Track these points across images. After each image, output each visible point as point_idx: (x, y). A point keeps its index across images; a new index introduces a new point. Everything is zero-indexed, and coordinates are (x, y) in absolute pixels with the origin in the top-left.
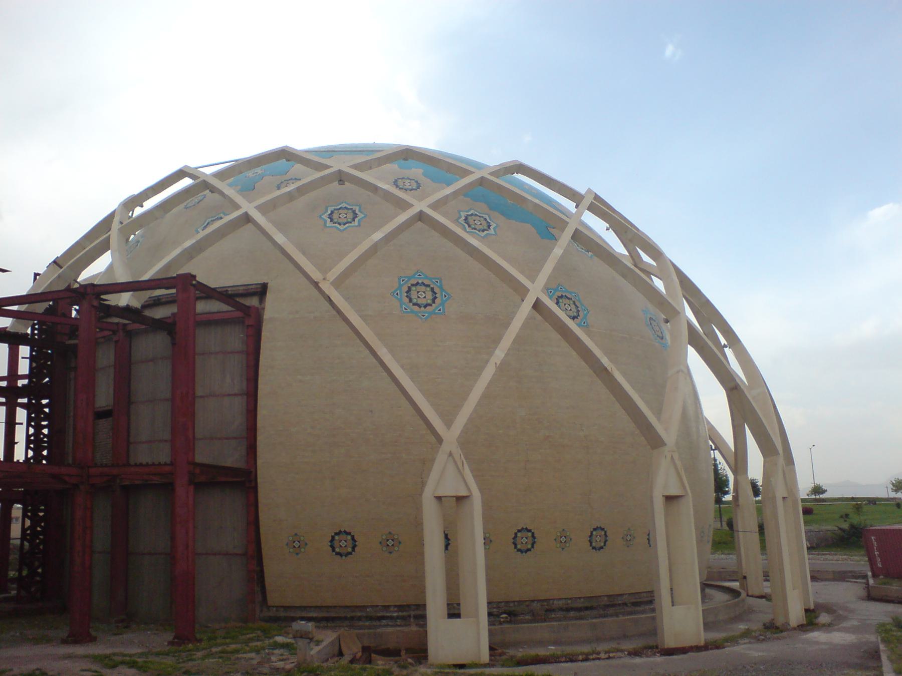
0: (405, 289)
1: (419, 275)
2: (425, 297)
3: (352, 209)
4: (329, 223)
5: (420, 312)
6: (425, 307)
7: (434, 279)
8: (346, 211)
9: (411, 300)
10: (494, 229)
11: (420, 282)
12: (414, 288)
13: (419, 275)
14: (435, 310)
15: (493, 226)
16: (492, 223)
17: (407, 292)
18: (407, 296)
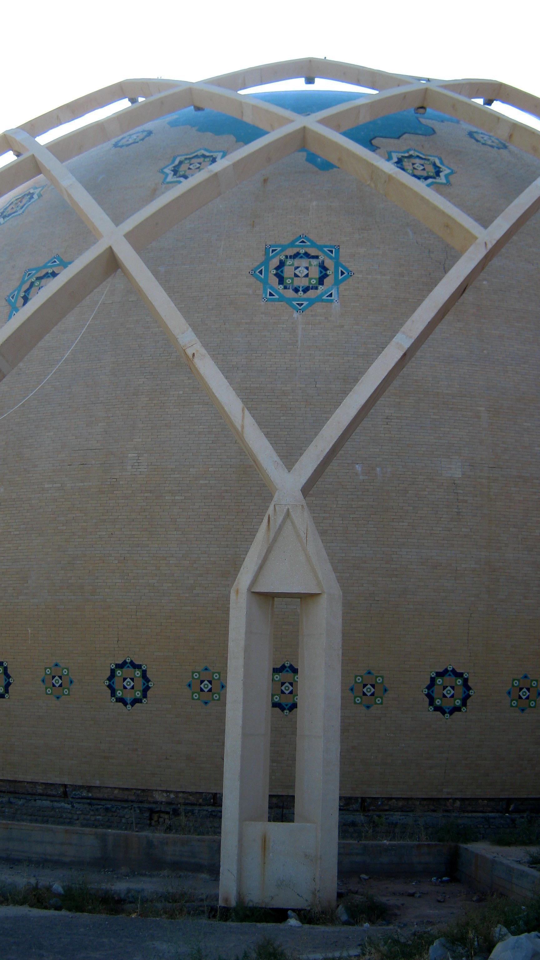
0: (275, 262)
1: (303, 242)
2: (307, 276)
3: (212, 156)
4: (170, 178)
5: (295, 299)
6: (306, 290)
7: (326, 247)
8: (201, 160)
9: (281, 280)
10: (447, 176)
11: (302, 251)
12: (289, 262)
13: (303, 242)
14: (322, 295)
15: (445, 171)
16: (443, 168)
17: (277, 268)
18: (276, 275)
